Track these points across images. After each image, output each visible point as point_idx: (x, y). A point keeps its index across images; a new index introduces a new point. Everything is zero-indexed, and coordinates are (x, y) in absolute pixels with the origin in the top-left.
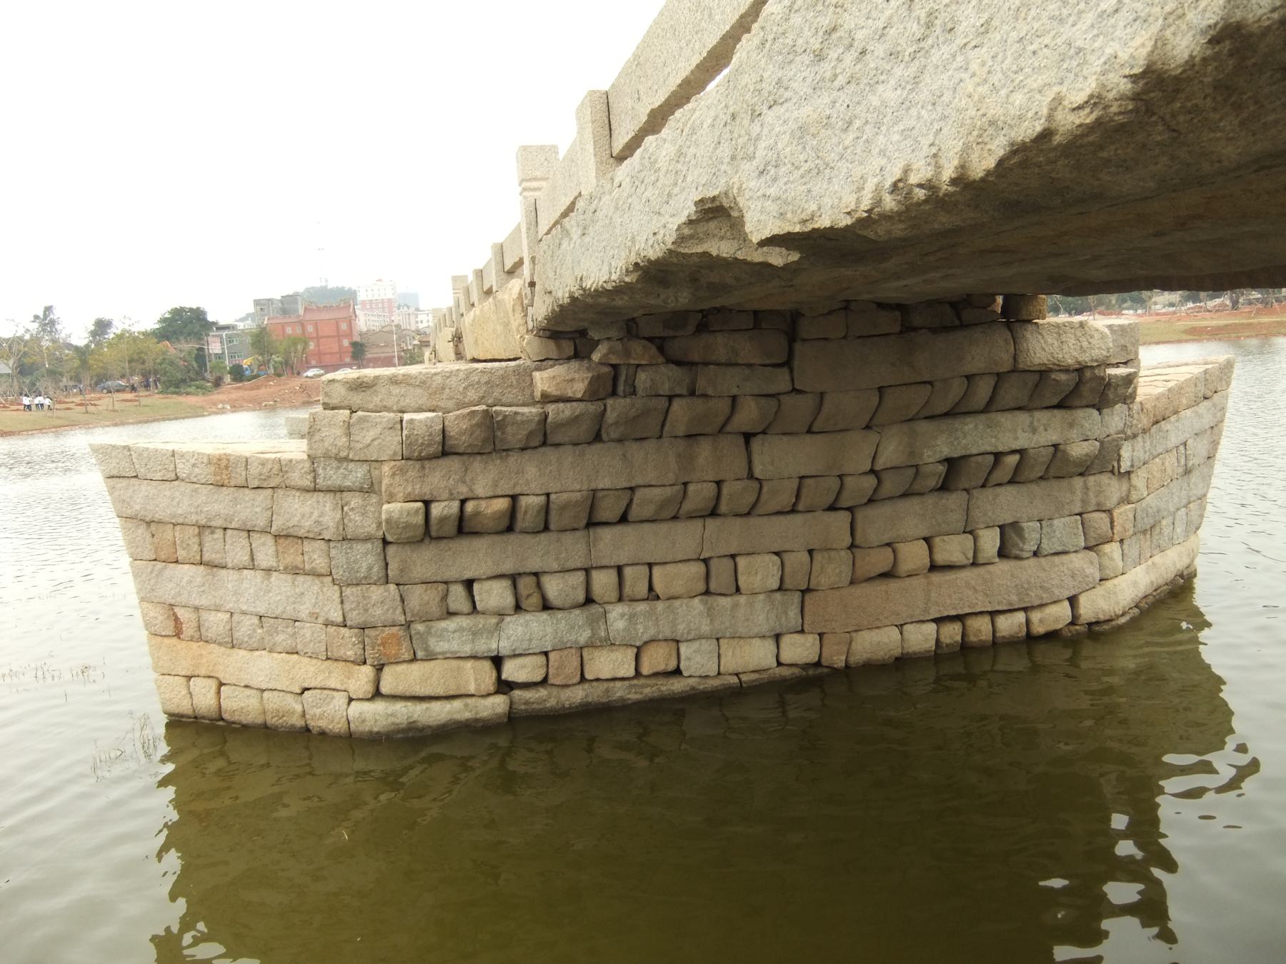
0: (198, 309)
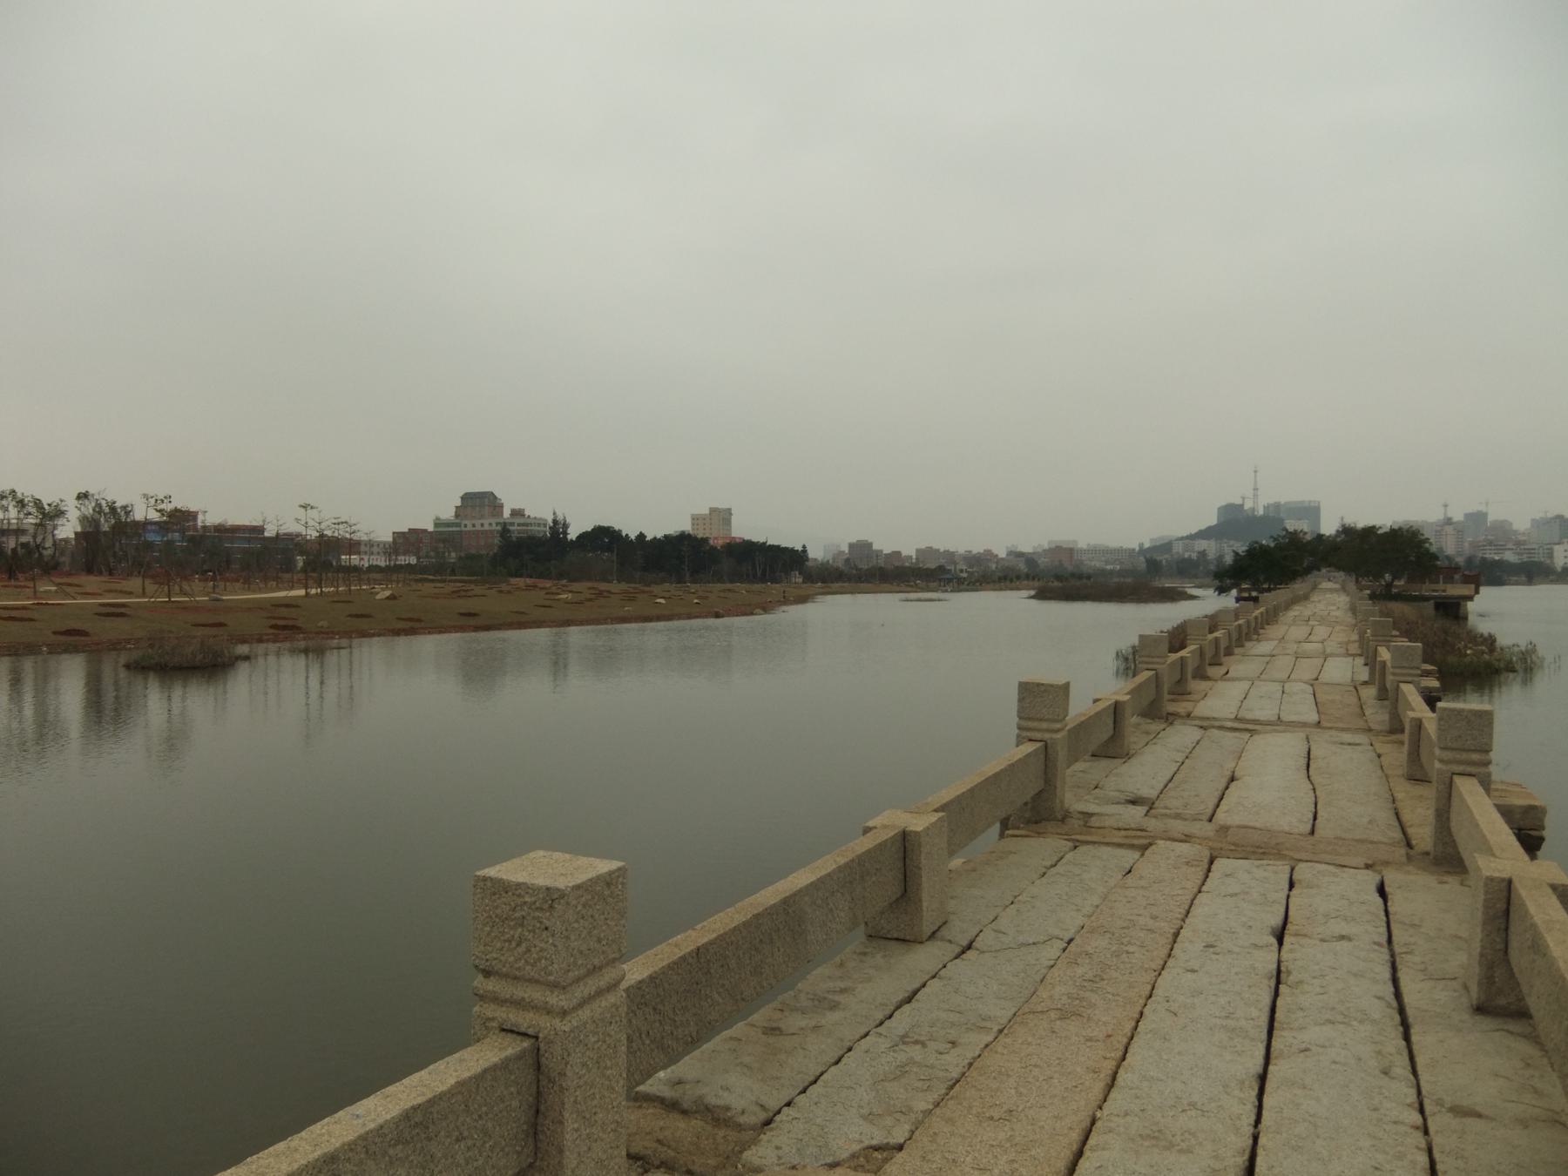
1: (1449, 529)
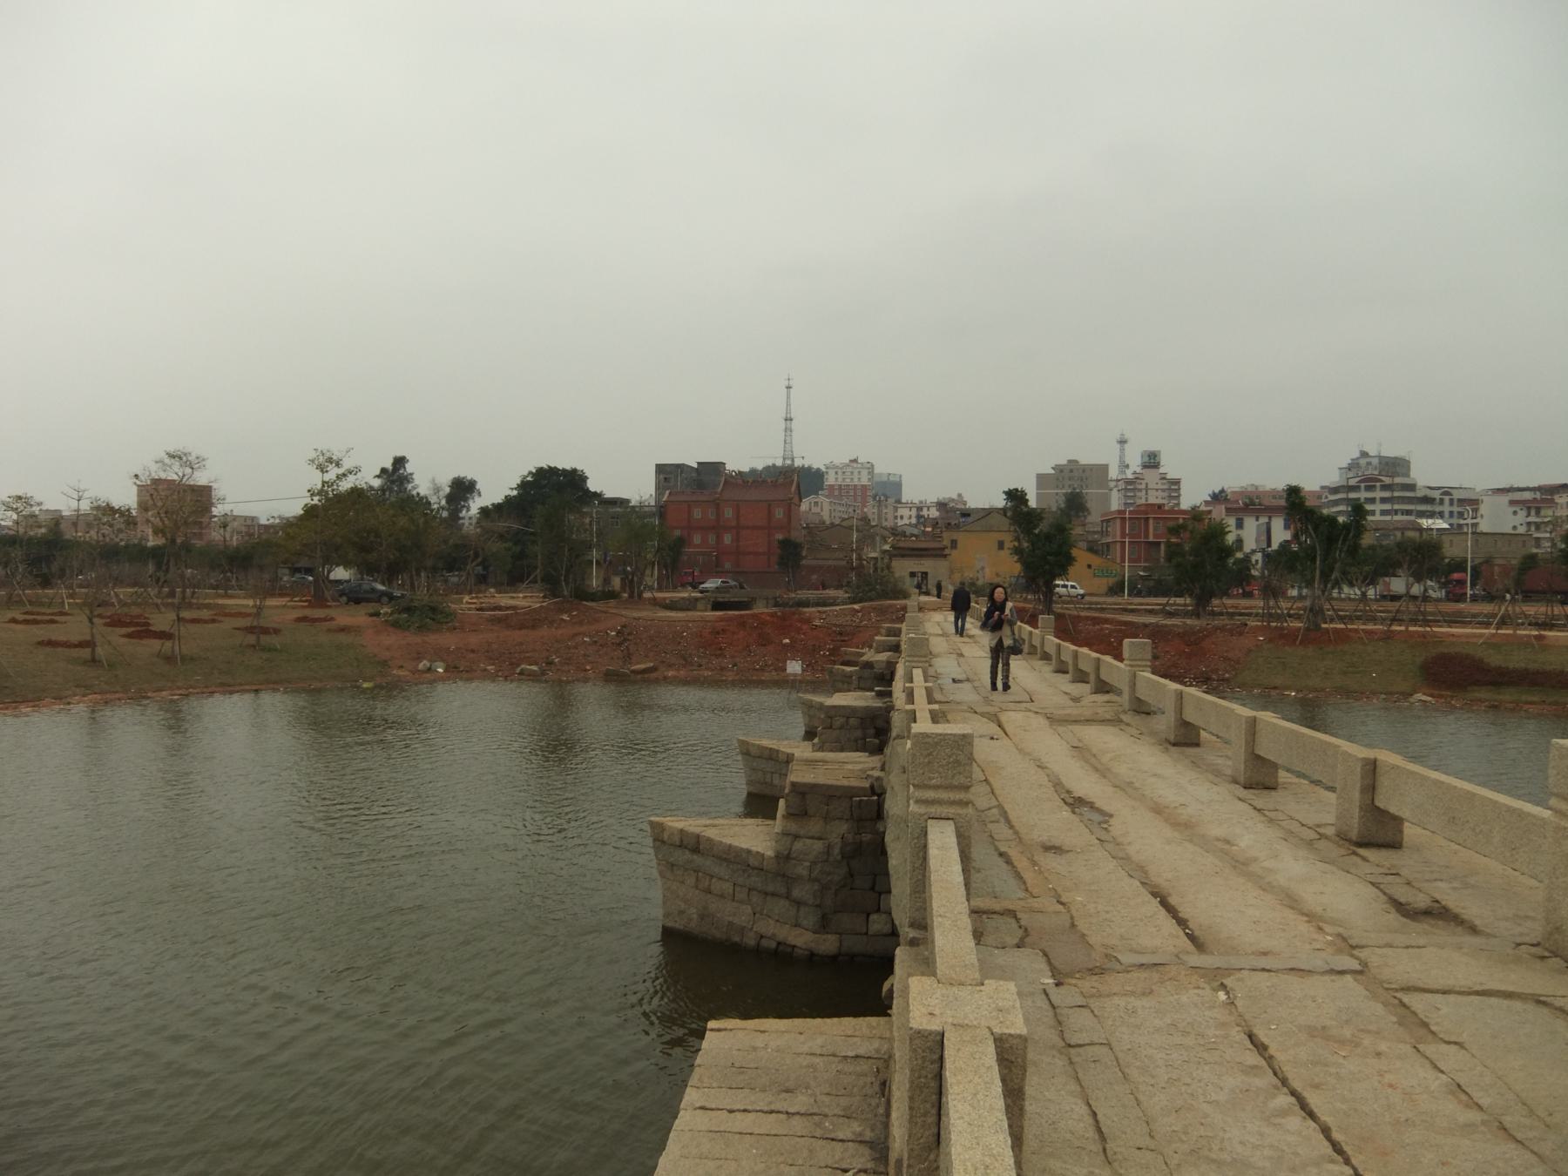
0: (574, 471)
1: (1151, 477)
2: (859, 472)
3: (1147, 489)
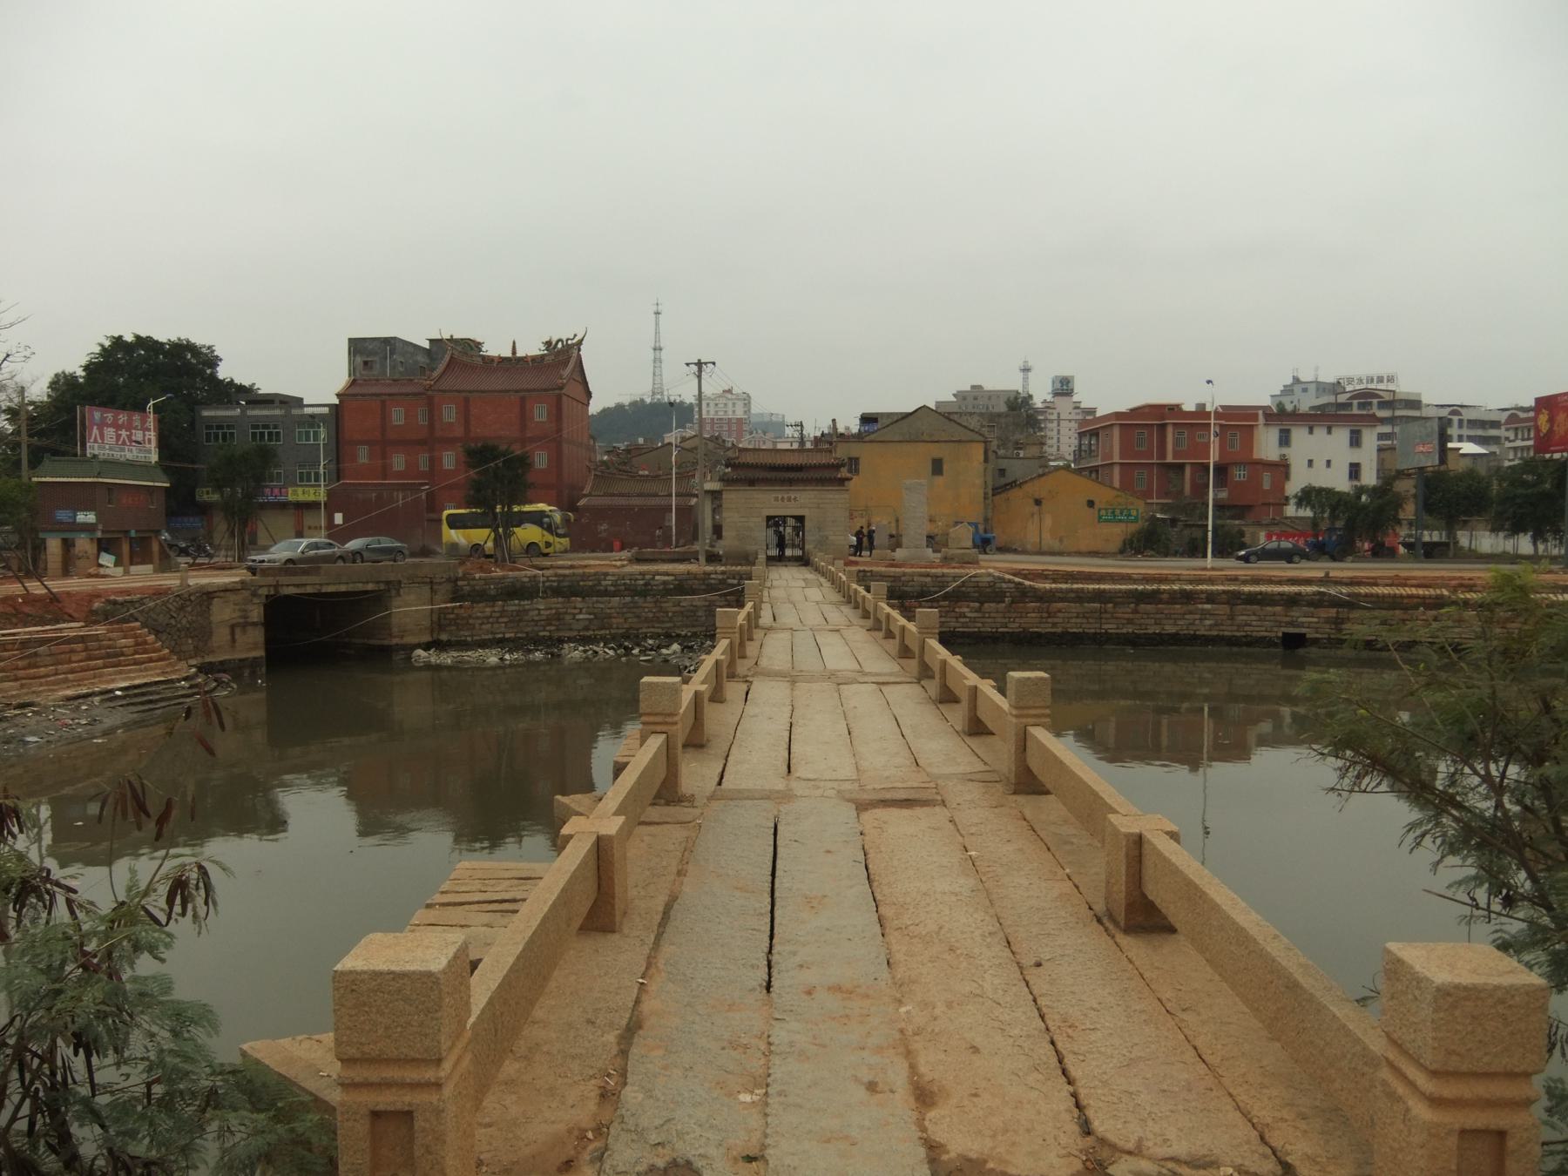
1: (1064, 405)
2: (734, 404)
3: (1059, 420)
